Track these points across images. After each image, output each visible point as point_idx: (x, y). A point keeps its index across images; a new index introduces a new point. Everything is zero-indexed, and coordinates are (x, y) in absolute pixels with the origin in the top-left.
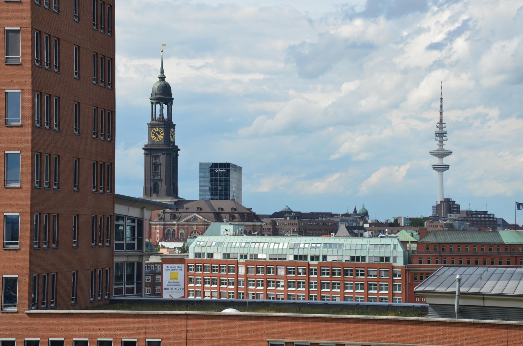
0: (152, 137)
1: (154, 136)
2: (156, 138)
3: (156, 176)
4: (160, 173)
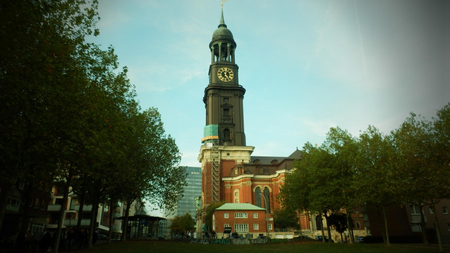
0: (219, 77)
1: (221, 76)
3: (227, 121)
4: (231, 117)
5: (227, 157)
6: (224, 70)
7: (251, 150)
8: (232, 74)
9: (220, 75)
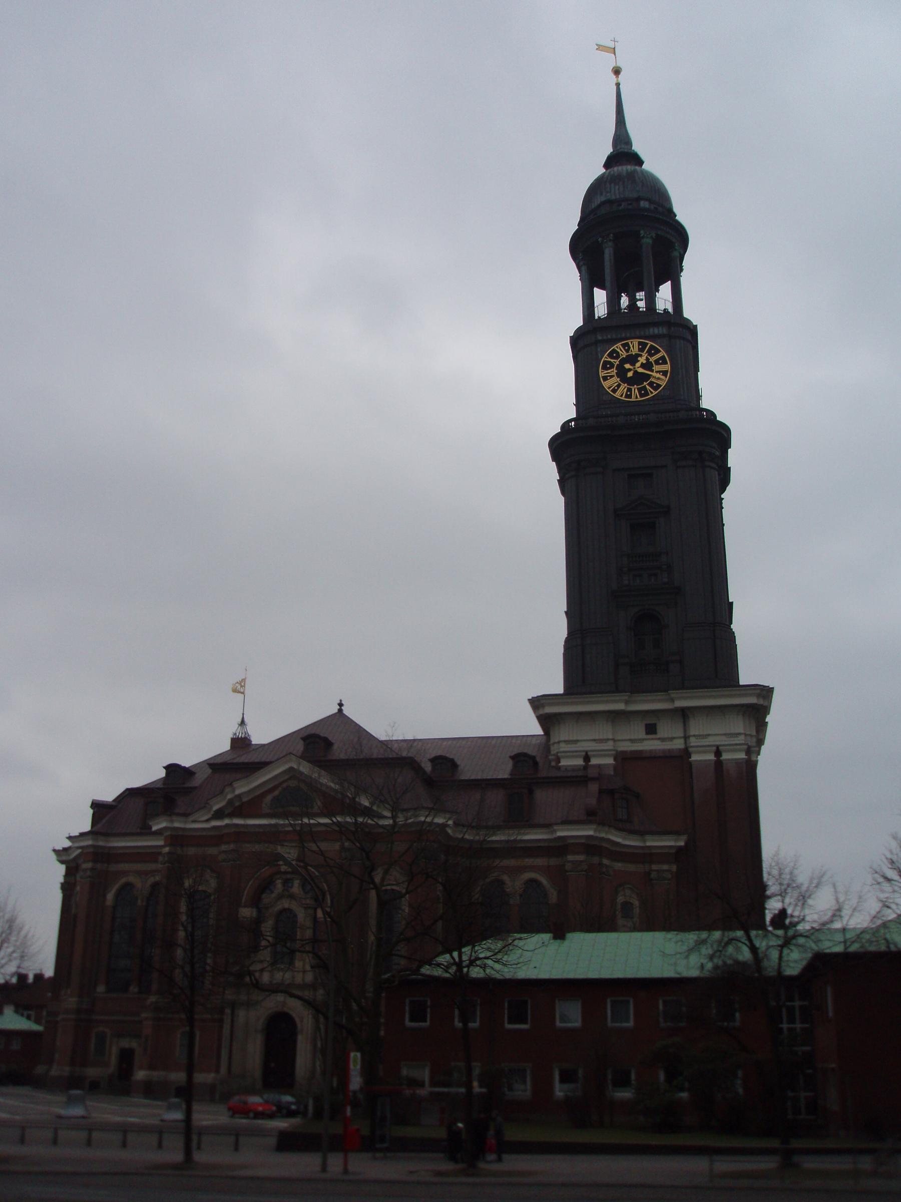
0: (605, 384)
1: (616, 380)
2: (629, 390)
5: (646, 743)
6: (627, 351)
7: (752, 700)
8: (665, 362)
9: (612, 377)
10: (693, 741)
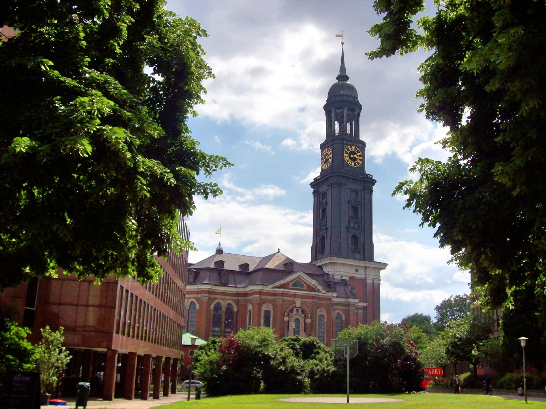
2: (351, 163)
4: (360, 219)
8: (361, 156)
10: (368, 276)
